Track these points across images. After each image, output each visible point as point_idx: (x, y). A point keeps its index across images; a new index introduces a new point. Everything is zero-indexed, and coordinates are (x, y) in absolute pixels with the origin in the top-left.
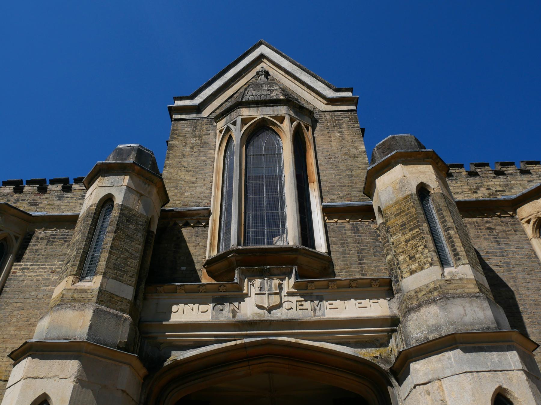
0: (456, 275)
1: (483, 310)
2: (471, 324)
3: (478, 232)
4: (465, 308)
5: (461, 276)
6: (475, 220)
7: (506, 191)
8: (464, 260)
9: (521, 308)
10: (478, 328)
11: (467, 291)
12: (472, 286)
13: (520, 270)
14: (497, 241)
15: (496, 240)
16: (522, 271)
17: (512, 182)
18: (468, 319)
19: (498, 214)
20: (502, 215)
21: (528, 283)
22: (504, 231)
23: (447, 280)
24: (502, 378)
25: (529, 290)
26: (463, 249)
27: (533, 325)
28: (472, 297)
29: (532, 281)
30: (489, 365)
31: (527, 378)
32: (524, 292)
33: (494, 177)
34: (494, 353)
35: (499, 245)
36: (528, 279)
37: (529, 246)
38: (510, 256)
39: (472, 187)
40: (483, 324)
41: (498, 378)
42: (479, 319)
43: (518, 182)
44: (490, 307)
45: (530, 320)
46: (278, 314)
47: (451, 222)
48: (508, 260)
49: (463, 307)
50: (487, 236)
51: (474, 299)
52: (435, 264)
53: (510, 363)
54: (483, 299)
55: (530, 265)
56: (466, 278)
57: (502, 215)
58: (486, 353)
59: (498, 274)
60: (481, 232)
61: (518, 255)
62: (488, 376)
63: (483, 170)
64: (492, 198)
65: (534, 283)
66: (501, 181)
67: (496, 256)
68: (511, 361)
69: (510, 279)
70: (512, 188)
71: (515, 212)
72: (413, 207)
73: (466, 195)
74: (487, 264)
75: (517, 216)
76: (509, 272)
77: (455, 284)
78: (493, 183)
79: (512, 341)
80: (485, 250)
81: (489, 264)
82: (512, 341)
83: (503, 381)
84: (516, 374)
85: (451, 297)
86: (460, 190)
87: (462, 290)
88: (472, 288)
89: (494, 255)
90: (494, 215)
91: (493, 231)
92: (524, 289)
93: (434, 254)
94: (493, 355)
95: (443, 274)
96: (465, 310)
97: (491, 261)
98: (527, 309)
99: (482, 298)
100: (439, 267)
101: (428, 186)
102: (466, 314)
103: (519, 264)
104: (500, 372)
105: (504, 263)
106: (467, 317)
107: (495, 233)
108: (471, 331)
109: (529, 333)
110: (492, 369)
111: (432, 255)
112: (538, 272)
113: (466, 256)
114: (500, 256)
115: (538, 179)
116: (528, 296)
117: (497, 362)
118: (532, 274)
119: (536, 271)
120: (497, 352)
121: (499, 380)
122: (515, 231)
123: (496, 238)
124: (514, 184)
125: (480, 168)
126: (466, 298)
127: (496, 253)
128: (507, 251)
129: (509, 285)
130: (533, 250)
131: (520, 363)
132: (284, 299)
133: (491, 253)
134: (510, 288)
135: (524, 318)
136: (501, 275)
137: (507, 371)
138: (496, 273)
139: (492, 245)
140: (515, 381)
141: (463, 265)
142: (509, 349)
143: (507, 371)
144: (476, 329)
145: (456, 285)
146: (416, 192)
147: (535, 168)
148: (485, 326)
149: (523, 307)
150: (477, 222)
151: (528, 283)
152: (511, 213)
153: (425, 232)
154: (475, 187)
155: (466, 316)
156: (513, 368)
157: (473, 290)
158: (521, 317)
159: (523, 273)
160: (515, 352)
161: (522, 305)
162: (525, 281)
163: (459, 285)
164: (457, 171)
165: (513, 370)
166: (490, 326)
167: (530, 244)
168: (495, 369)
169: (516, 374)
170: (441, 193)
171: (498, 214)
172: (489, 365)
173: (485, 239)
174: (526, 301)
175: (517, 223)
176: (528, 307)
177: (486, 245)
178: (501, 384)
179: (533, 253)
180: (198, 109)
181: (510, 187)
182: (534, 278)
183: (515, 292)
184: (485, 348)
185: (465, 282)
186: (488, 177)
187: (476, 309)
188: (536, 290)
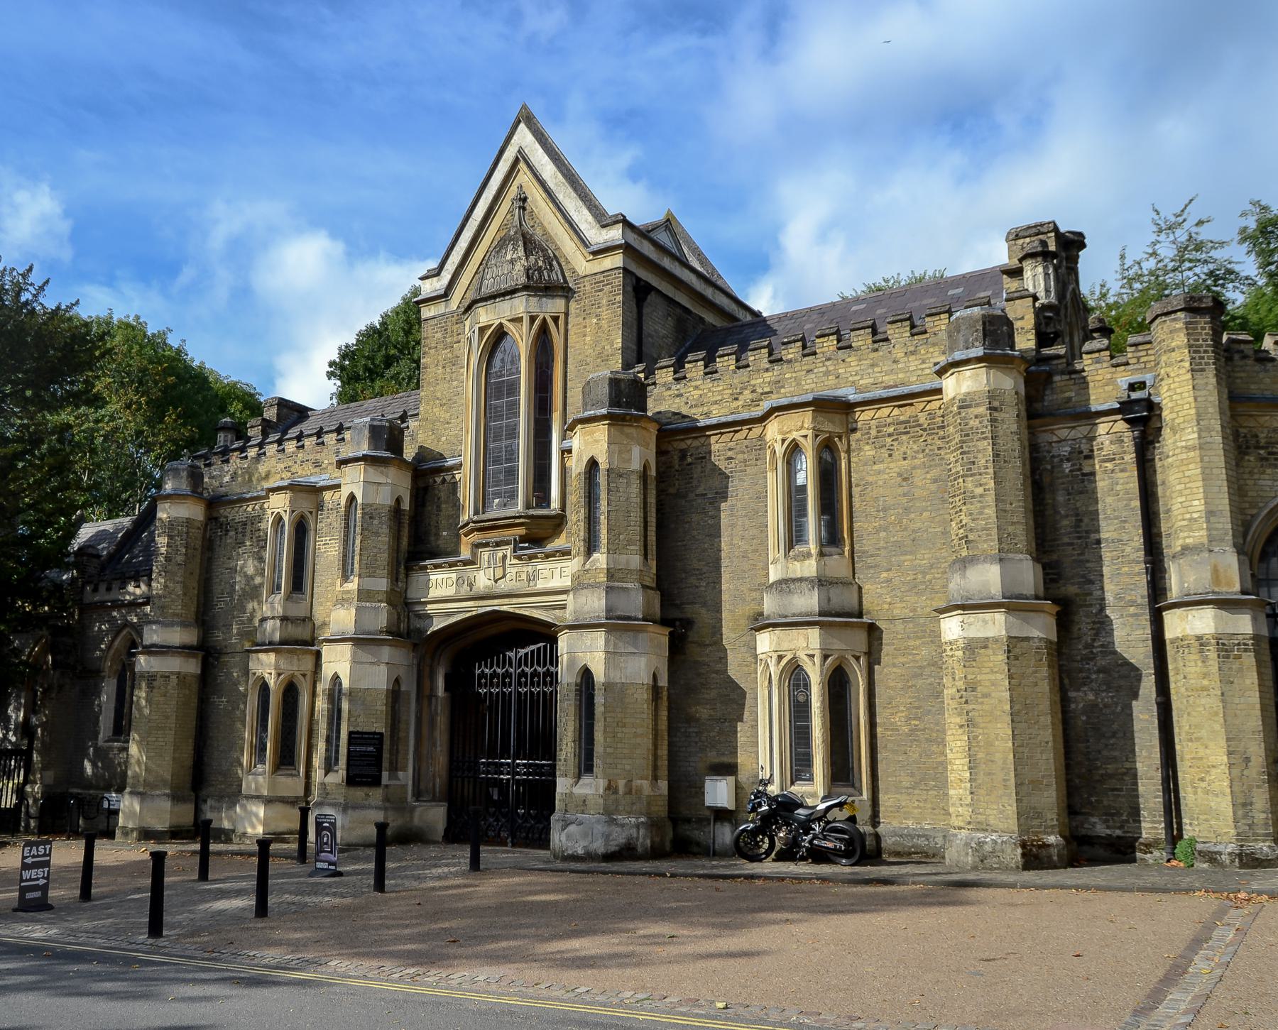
1: (600, 599)
22: (745, 461)
33: (767, 370)
43: (794, 375)
46: (503, 586)
61: (748, 494)
70: (783, 387)
86: (720, 398)
107: (733, 465)
116: (739, 547)
132: (508, 570)
167: (766, 478)
180: (446, 295)
181: (781, 384)
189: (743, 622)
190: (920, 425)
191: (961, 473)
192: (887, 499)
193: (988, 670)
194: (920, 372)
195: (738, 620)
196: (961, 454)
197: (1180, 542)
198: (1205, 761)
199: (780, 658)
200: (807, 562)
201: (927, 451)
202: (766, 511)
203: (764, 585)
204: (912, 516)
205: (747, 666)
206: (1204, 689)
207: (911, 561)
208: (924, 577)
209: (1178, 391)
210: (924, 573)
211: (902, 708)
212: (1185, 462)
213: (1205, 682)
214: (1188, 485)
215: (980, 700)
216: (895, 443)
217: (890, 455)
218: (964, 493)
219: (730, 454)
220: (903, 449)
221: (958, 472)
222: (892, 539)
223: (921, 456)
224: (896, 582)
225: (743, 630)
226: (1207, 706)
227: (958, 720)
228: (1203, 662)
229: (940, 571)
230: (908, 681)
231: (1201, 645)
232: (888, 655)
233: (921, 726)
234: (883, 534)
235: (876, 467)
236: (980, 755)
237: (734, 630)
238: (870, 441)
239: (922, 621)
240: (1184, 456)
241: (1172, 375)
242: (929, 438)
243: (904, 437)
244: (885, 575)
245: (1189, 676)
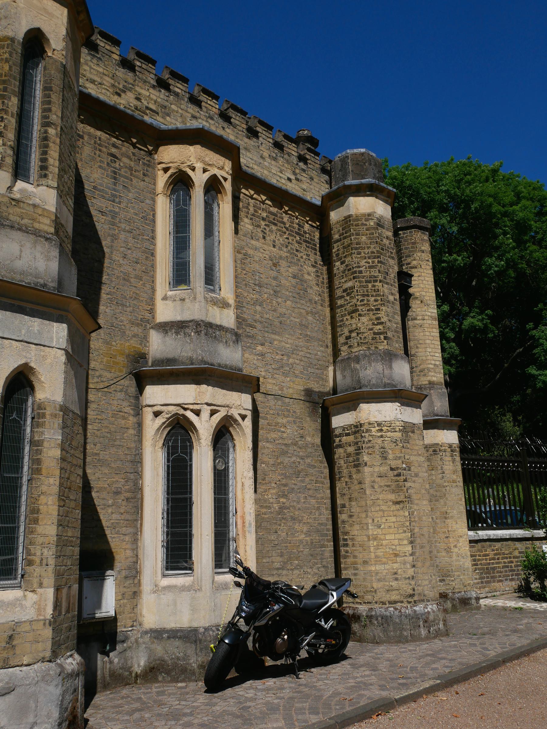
0: (31, 197)
1: (48, 259)
2: (22, 273)
3: (95, 154)
4: (22, 248)
5: (37, 201)
6: (99, 133)
7: (160, 114)
8: (52, 180)
9: (105, 278)
10: (29, 281)
11: (37, 225)
12: (47, 221)
13: (127, 229)
14: (115, 178)
15: (115, 175)
16: (128, 232)
17: (173, 107)
18: (19, 264)
19: (134, 141)
20: (137, 145)
21: (129, 249)
22: (131, 169)
23: (13, 199)
24: (33, 354)
25: (125, 258)
26: (57, 163)
27: (109, 303)
28: (40, 236)
29: (134, 248)
30: (23, 333)
31: (66, 361)
32: (118, 259)
33: (154, 87)
34: (36, 319)
35: (115, 184)
36: (130, 244)
37: (152, 202)
38: (122, 206)
39: (116, 84)
40: (39, 278)
41: (28, 352)
42: (37, 269)
43: (180, 111)
44: (59, 259)
45: (109, 296)
47: (57, 116)
48: (117, 210)
49: (21, 246)
50: (105, 165)
51: (42, 240)
52: (4, 168)
53: (52, 338)
54: (55, 244)
55: (141, 227)
56: (43, 207)
57: (137, 145)
58: (26, 317)
59: (96, 224)
60: (99, 156)
61: (133, 208)
62: (15, 347)
63: (144, 66)
64: (137, 114)
65: (135, 252)
66: (159, 97)
67: (104, 197)
68: (54, 335)
69: (109, 235)
70: (168, 115)
71: (156, 150)
72: (7, 61)
73: (104, 91)
74: (88, 204)
75: (156, 156)
76: (111, 226)
77: (23, 209)
78: (148, 94)
79: (67, 311)
80: (94, 183)
81: (90, 204)
82: (67, 311)
83: (33, 358)
84: (54, 353)
85: (8, 226)
87: (30, 221)
88: (46, 224)
89: (103, 196)
90: (128, 140)
91: (115, 162)
92: (119, 255)
93: (10, 152)
94: (34, 322)
95: (10, 188)
96: (21, 251)
97: (94, 201)
98: (112, 281)
99: (54, 242)
100: (10, 175)
101: (48, 40)
102: (20, 257)
103: (129, 221)
104: (34, 346)
105: (111, 211)
106: (21, 262)
108: (18, 281)
109: (100, 311)
110: (25, 339)
111: (5, 152)
112: (146, 239)
113: (57, 176)
114: (110, 201)
115: (205, 119)
116: (120, 265)
117: (36, 331)
118: (138, 239)
119: (145, 237)
120: (41, 320)
121: (28, 354)
122: (144, 175)
123: (115, 173)
124: (173, 110)
125: (141, 63)
126: (31, 235)
127: (107, 194)
128: (122, 197)
129: (104, 243)
130: (154, 210)
131: (66, 341)
133: (100, 190)
134: (102, 247)
135: (103, 291)
136: (98, 226)
137: (44, 346)
138: (93, 221)
139: (106, 180)
140: (49, 361)
141: (47, 186)
142: (59, 320)
143: (44, 346)
144: (26, 281)
145: (24, 211)
146: (23, 39)
147: (209, 102)
148: (41, 281)
149: (107, 277)
150: (100, 139)
151: (129, 249)
152: (151, 148)
153: (10, 111)
154: (121, 86)
155: (20, 260)
156: (54, 344)
157: (46, 228)
158: (100, 289)
159: (128, 235)
160: (65, 326)
161: (108, 275)
162: (125, 245)
163: (29, 213)
164: (108, 47)
165: (53, 347)
166: (48, 284)
167: (154, 201)
168: (29, 341)
169: (54, 353)
170: (62, 63)
171: (134, 141)
172: (23, 333)
173: (100, 167)
174: (115, 271)
175: (151, 165)
176: (114, 279)
177: (97, 176)
178: (29, 361)
179: (152, 214)
181: (167, 111)
182: (139, 246)
183: (107, 255)
184: (28, 310)
185: (40, 211)
186: (145, 82)
187: (38, 255)
188: (133, 261)
189: (121, 359)
190: (284, 223)
191: (380, 278)
192: (262, 276)
193: (415, 453)
194: (278, 178)
195: (115, 356)
196: (379, 262)
197: (429, 378)
198: (456, 532)
199: (213, 413)
200: (226, 311)
201: (289, 248)
202: (154, 238)
203: (148, 321)
204: (279, 300)
205: (124, 418)
206: (454, 481)
207: (280, 341)
208: (288, 360)
209: (427, 279)
210: (289, 357)
211: (273, 485)
212: (431, 326)
213: (455, 477)
214: (433, 342)
215: (414, 479)
216: (268, 229)
217: (264, 238)
218: (383, 296)
219: (113, 150)
220: (273, 237)
221: (375, 277)
222: (265, 316)
223: (285, 250)
224: (268, 356)
225: (120, 371)
226: (456, 493)
227: (392, 497)
228: (453, 463)
229: (299, 357)
230: (277, 459)
231: (452, 451)
232: (263, 428)
233: (287, 504)
234: (258, 308)
235: (253, 242)
236: (417, 530)
237: (108, 368)
238: (249, 216)
239: (287, 400)
240: (430, 322)
241: (423, 267)
242: (290, 238)
243: (274, 228)
244: (259, 348)
245: (446, 472)
